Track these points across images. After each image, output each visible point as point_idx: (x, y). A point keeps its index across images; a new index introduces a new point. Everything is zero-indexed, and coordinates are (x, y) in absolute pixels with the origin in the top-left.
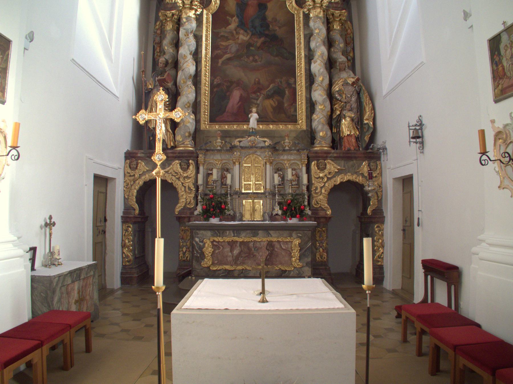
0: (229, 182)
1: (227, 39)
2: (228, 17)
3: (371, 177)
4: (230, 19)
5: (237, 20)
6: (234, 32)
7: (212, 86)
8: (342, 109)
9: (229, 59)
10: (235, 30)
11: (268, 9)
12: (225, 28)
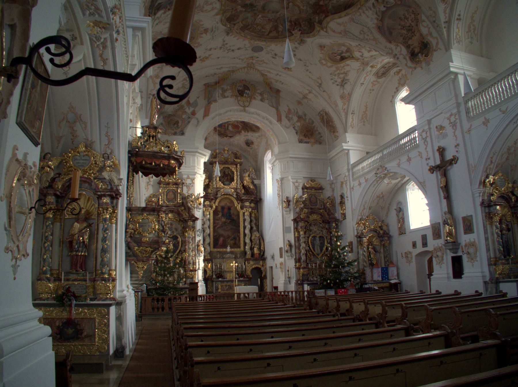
0: (223, 268)
1: (218, 220)
3: (263, 266)
7: (214, 236)
8: (255, 244)
9: (219, 227)
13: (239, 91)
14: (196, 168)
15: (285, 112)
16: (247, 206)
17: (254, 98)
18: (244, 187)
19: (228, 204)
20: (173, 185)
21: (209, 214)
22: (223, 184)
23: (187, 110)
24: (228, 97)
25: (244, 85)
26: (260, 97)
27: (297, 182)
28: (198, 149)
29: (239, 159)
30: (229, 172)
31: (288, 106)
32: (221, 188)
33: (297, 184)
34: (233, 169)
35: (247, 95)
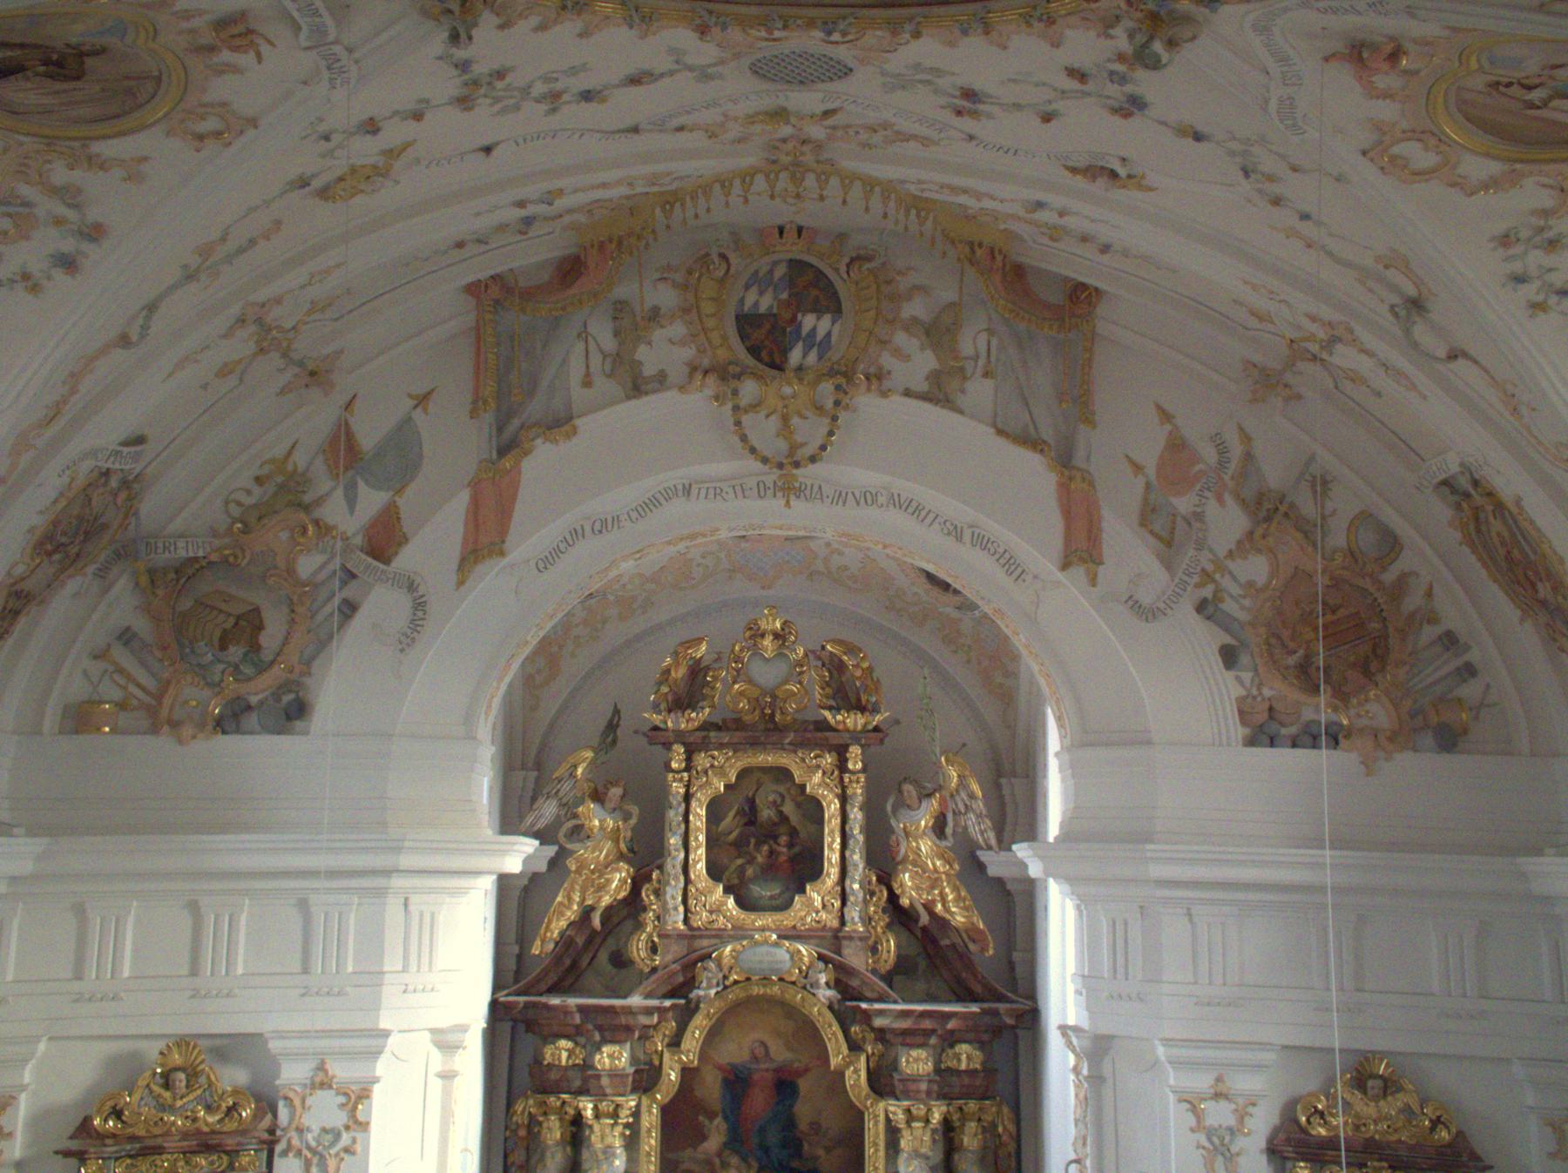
2: (701, 1118)
4: (707, 1122)
5: (724, 1126)
6: (717, 1161)
10: (719, 1155)
11: (801, 1094)
12: (695, 1148)
13: (747, 322)
14: (390, 992)
15: (1137, 468)
16: (915, 1079)
17: (877, 378)
18: (900, 915)
19: (780, 1054)
20: (188, 1153)
21: (632, 1143)
22: (742, 903)
23: (334, 511)
24: (661, 380)
25: (797, 266)
26: (919, 363)
27: (1217, 1096)
28: (398, 850)
29: (862, 709)
30: (788, 808)
31: (1166, 416)
32: (721, 936)
33: (1219, 1114)
34: (816, 783)
35: (812, 357)
